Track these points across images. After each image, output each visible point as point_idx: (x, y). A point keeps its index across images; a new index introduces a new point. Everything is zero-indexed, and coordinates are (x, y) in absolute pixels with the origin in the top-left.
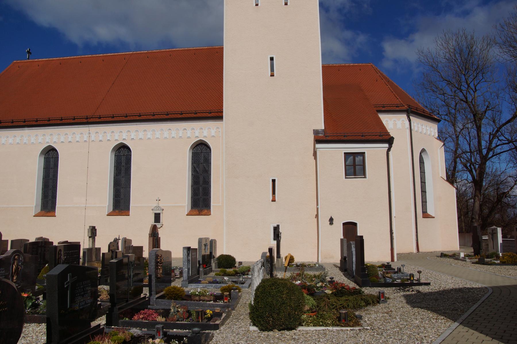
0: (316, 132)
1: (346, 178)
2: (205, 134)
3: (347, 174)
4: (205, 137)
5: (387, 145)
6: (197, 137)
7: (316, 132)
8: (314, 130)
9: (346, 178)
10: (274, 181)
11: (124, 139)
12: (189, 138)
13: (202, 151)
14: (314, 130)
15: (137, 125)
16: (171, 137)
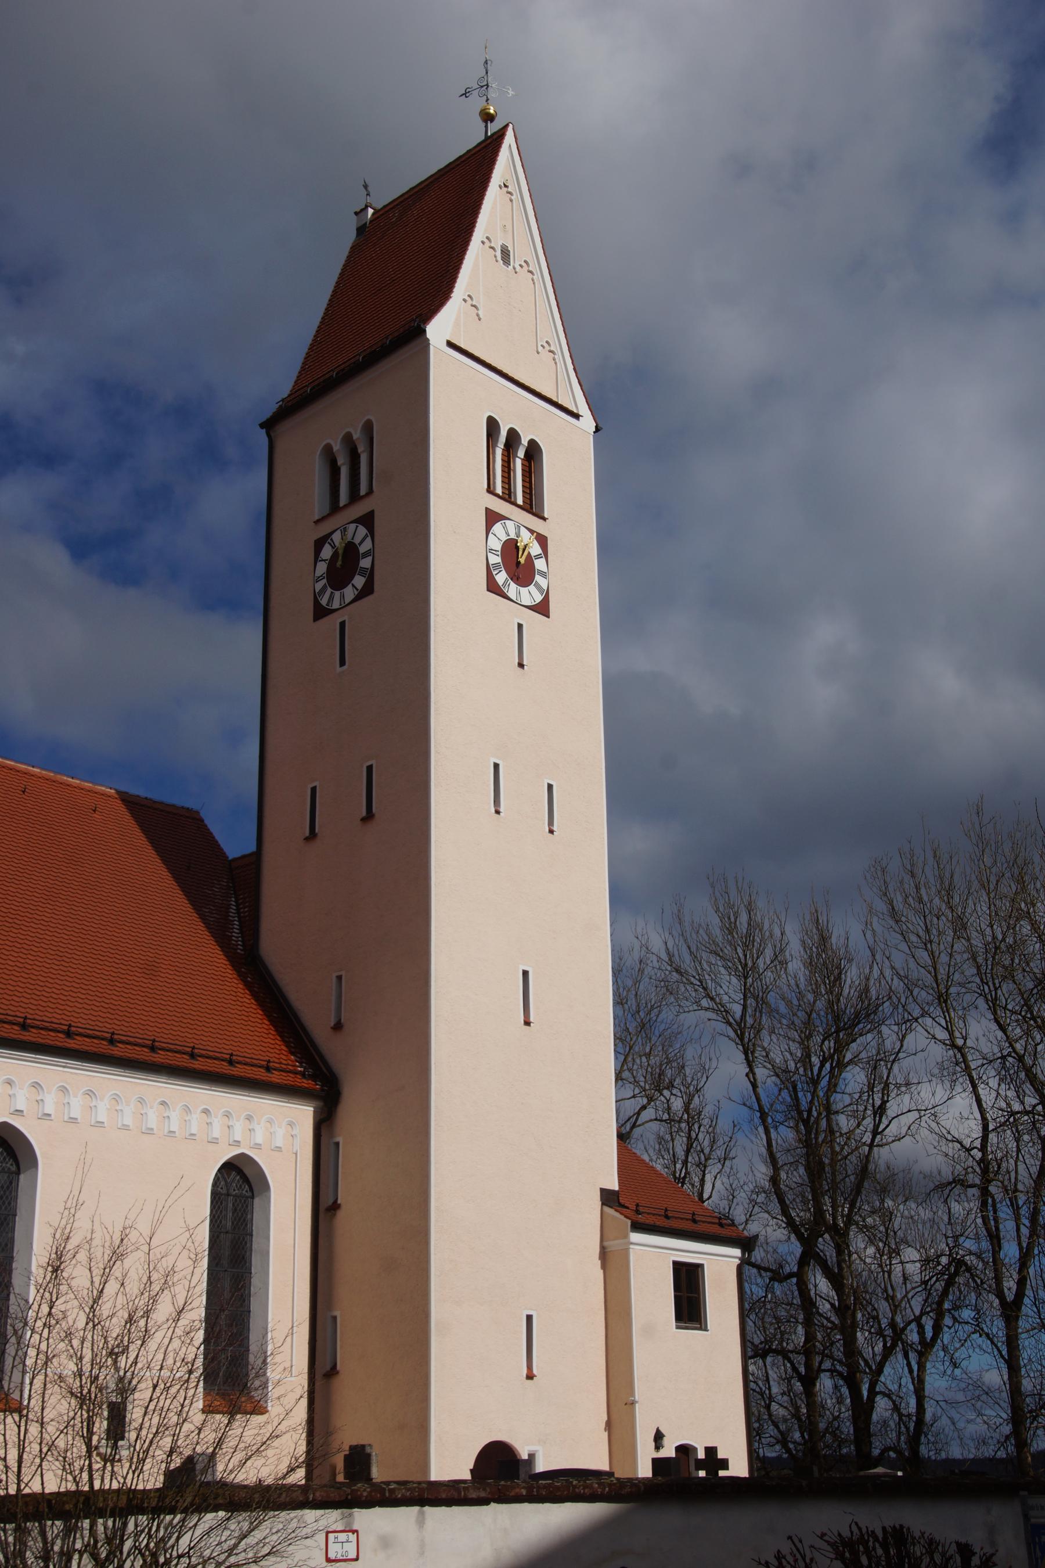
0: (608, 1198)
1: (678, 1327)
2: (259, 1138)
3: (679, 1317)
4: (258, 1147)
5: (737, 1252)
6: (237, 1143)
7: (608, 1198)
8: (602, 1190)
9: (678, 1327)
10: (529, 1318)
11: (19, 1112)
12: (215, 1141)
13: (228, 1190)
14: (602, 1190)
15: (64, 1067)
16: (166, 1131)
